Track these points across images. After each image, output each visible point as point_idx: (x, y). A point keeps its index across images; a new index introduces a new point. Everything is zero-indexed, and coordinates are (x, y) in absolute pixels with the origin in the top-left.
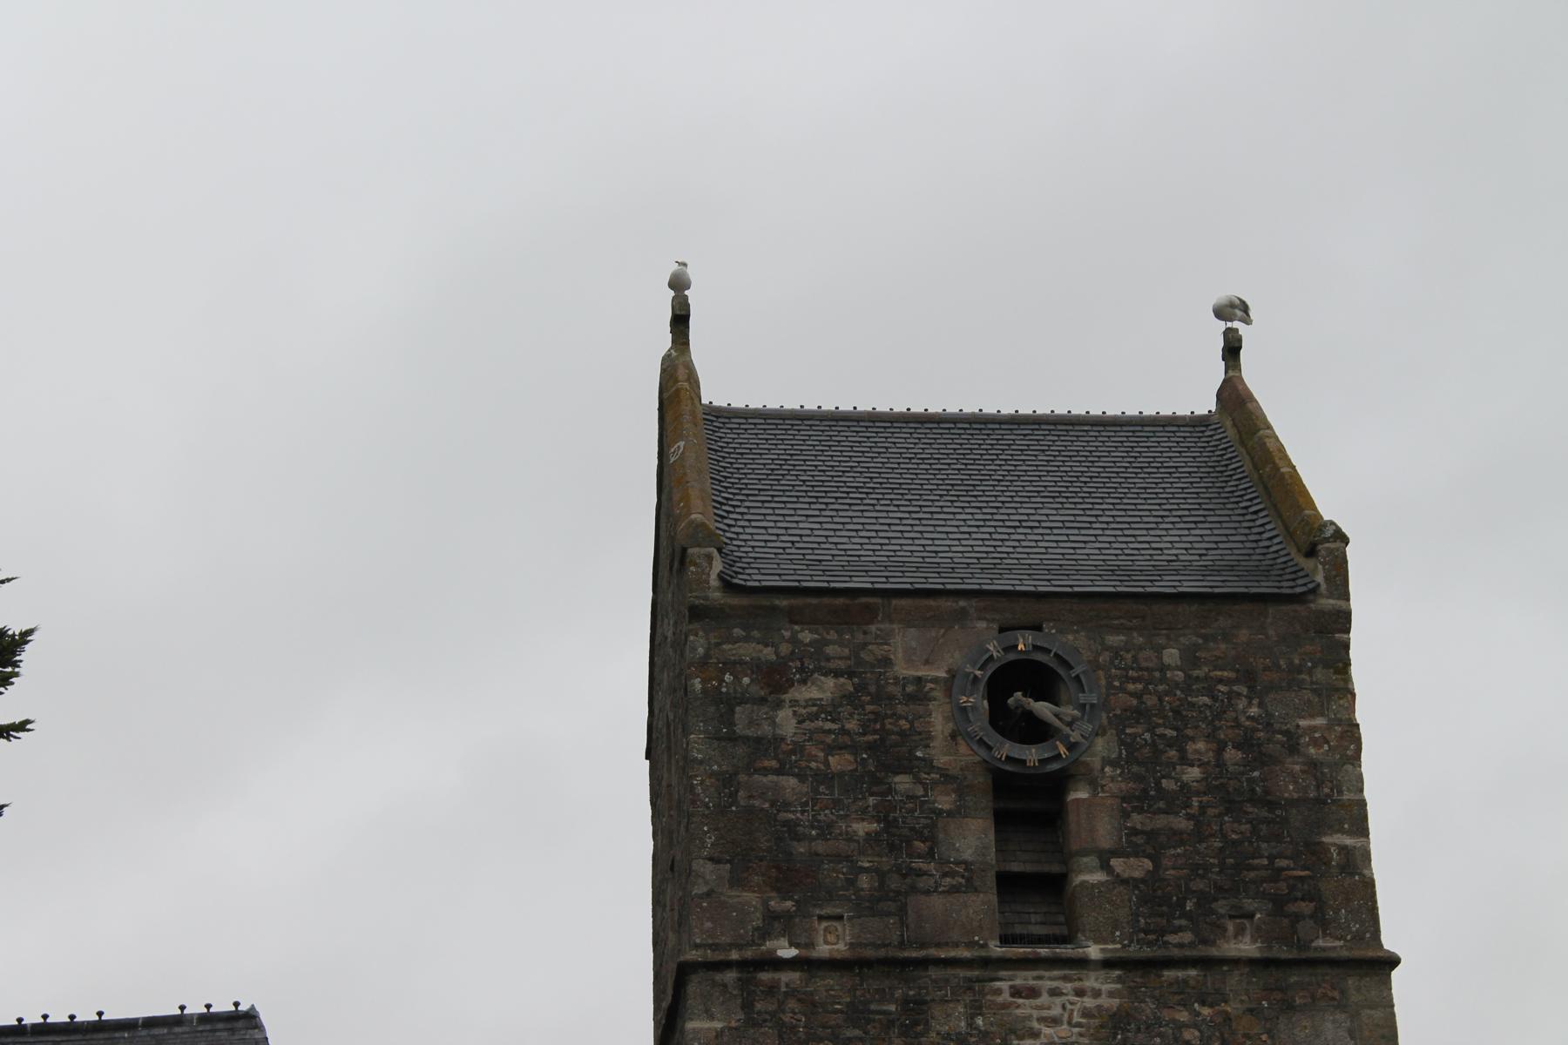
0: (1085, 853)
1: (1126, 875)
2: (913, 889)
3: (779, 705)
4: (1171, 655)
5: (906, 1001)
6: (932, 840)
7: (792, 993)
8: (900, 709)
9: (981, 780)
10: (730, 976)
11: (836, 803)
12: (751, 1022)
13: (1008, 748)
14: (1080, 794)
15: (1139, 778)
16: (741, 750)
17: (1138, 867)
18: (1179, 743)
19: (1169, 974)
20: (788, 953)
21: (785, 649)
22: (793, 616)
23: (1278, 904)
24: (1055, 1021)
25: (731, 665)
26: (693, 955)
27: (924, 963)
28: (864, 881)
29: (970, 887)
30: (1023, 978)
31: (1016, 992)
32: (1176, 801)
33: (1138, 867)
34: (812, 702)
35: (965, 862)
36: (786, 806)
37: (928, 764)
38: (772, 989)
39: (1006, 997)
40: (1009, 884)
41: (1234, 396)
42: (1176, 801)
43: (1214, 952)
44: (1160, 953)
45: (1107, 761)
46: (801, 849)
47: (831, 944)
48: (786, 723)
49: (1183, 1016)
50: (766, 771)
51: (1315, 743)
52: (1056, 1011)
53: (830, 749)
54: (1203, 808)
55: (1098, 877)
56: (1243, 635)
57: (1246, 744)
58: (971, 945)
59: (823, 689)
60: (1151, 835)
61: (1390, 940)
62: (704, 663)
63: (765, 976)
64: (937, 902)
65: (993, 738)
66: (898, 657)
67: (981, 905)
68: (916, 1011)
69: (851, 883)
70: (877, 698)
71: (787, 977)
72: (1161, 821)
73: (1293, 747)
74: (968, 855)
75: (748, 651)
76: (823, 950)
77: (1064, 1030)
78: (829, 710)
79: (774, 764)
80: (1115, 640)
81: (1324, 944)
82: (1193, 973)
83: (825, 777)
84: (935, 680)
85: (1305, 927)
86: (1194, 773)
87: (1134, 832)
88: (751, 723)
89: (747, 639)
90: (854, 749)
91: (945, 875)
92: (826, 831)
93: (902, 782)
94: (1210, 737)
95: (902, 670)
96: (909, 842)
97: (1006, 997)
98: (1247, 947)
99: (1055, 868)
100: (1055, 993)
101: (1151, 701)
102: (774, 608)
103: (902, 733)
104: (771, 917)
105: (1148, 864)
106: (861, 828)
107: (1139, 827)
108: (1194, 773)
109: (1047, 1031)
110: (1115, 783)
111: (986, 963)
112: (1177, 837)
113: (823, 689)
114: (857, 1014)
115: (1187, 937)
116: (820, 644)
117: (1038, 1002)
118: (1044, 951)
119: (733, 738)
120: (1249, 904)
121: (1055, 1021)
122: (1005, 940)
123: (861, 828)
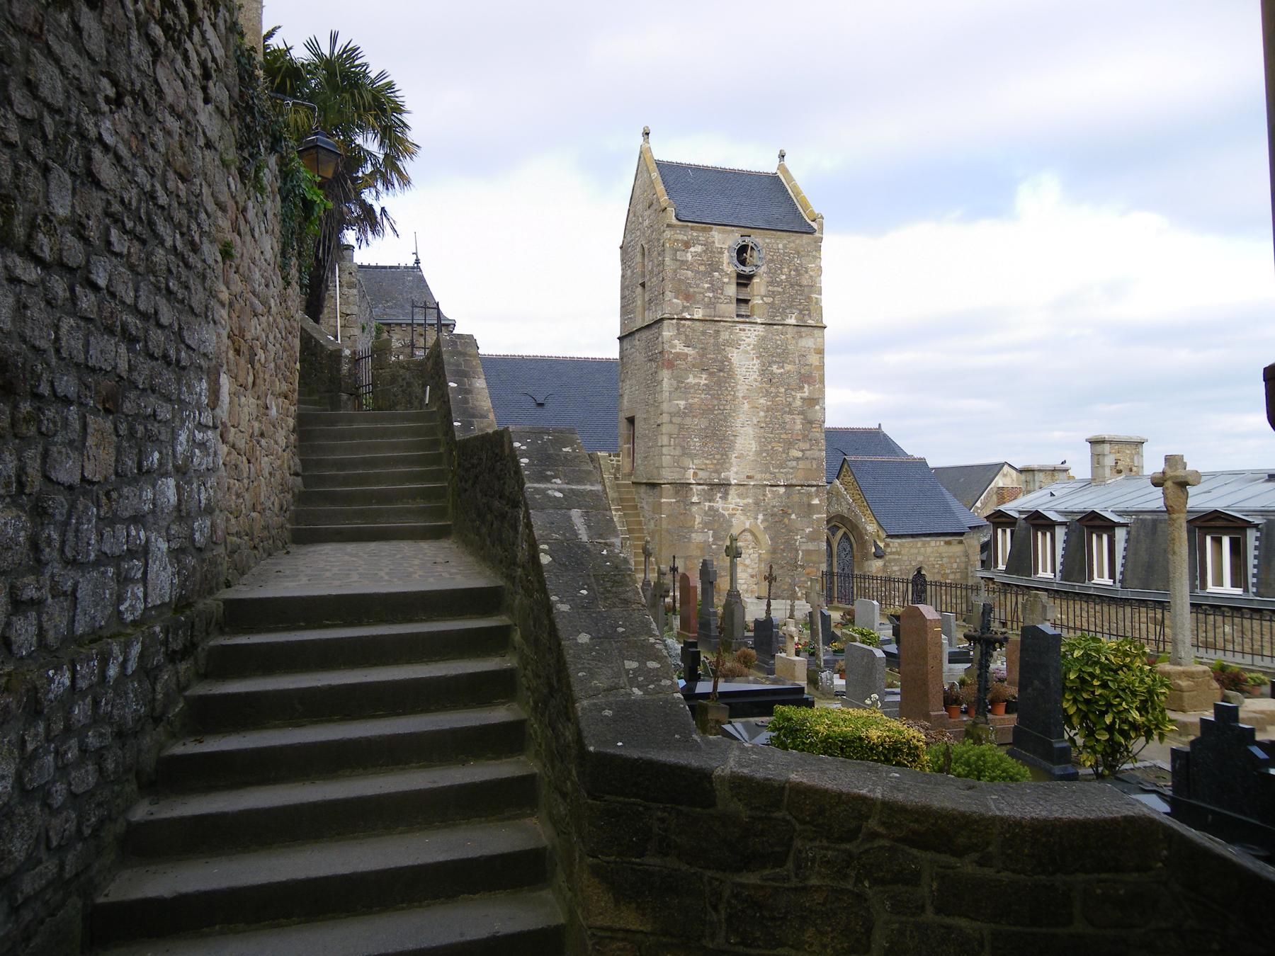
3: (687, 252)
4: (780, 246)
6: (722, 290)
7: (689, 327)
8: (716, 255)
9: (735, 275)
10: (675, 321)
11: (700, 279)
13: (742, 268)
14: (756, 280)
15: (771, 277)
16: (678, 263)
17: (769, 300)
18: (781, 269)
19: (775, 327)
20: (689, 317)
21: (689, 237)
22: (692, 229)
23: (801, 311)
24: (749, 337)
25: (677, 240)
26: (666, 316)
27: (721, 321)
28: (706, 299)
29: (731, 303)
30: (742, 326)
31: (740, 330)
32: (779, 284)
33: (769, 300)
34: (695, 252)
36: (688, 279)
38: (684, 325)
39: (738, 331)
40: (739, 301)
41: (782, 167)
42: (779, 284)
43: (786, 323)
44: (773, 322)
45: (764, 272)
46: (691, 290)
47: (699, 314)
48: (689, 257)
49: (778, 338)
50: (684, 269)
51: (811, 271)
53: (699, 265)
54: (785, 286)
55: (761, 302)
56: (797, 242)
57: (796, 270)
58: (730, 317)
59: (699, 249)
60: (773, 292)
61: (825, 322)
62: (670, 239)
63: (683, 322)
64: (723, 306)
65: (739, 265)
66: (716, 242)
67: (733, 307)
68: (717, 332)
70: (711, 252)
71: (688, 323)
72: (776, 289)
73: (807, 272)
74: (730, 294)
75: (680, 237)
76: (696, 317)
80: (767, 241)
81: (810, 322)
82: (780, 327)
83: (698, 272)
85: (806, 317)
86: (784, 277)
89: (680, 234)
90: (705, 265)
92: (698, 286)
93: (716, 274)
94: (788, 268)
95: (717, 245)
97: (738, 331)
98: (792, 321)
99: (749, 298)
100: (749, 330)
101: (775, 257)
102: (688, 226)
104: (684, 307)
106: (706, 286)
108: (784, 277)
109: (747, 340)
110: (766, 278)
111: (734, 322)
112: (779, 293)
113: (699, 249)
114: (704, 333)
115: (779, 318)
116: (698, 236)
118: (747, 320)
119: (677, 260)
120: (794, 311)
121: (749, 337)
122: (738, 316)
123: (706, 286)
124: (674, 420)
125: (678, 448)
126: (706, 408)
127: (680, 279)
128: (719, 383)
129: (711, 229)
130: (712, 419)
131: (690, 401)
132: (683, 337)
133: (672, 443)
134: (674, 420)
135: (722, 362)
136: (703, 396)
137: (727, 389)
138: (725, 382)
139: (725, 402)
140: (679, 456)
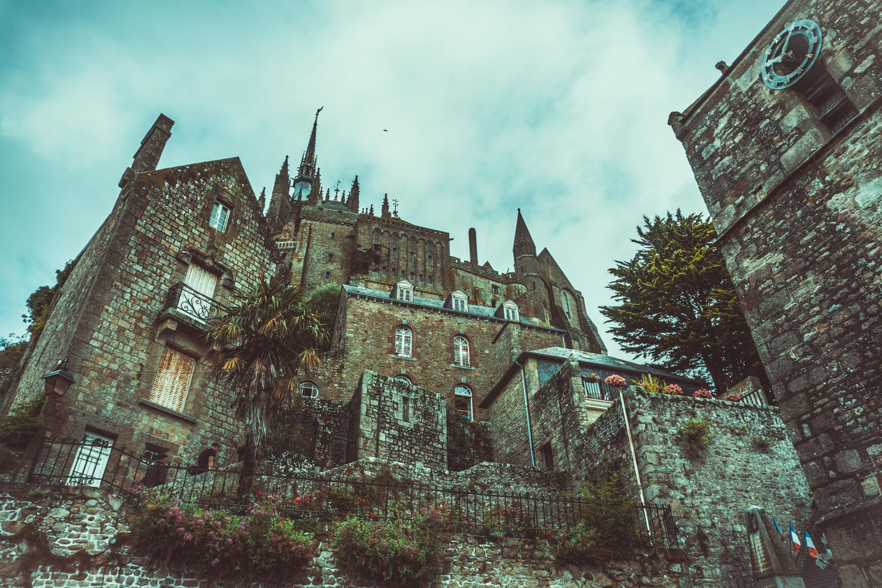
0: (841, 80)
1: (864, 70)
2: (781, 154)
3: (713, 140)
5: (794, 195)
12: (744, 247)
21: (708, 123)
25: (696, 143)
35: (795, 128)
37: (767, 110)
50: (717, 163)
52: (859, 146)
53: (733, 138)
59: (723, 122)
60: (868, 44)
64: (791, 152)
68: (801, 194)
69: (758, 172)
70: (740, 108)
74: (795, 124)
77: (866, 152)
78: (729, 125)
79: (719, 158)
83: (736, 147)
84: (756, 83)
87: (859, 51)
88: (707, 153)
90: (741, 130)
91: (789, 140)
92: (742, 164)
95: (744, 89)
96: (772, 140)
100: (854, 142)
102: (699, 114)
103: (754, 109)
105: (873, 56)
107: (859, 48)
113: (723, 122)
114: (778, 216)
117: (849, 150)
124: (794, 387)
125: (822, 437)
126: (836, 331)
127: (718, 179)
128: (845, 268)
129: (727, 85)
130: (864, 343)
131: (807, 337)
132: (753, 247)
133: (807, 432)
134: (794, 387)
135: (831, 229)
136: (825, 313)
137: (866, 269)
138: (855, 260)
139: (873, 296)
140: (831, 454)
